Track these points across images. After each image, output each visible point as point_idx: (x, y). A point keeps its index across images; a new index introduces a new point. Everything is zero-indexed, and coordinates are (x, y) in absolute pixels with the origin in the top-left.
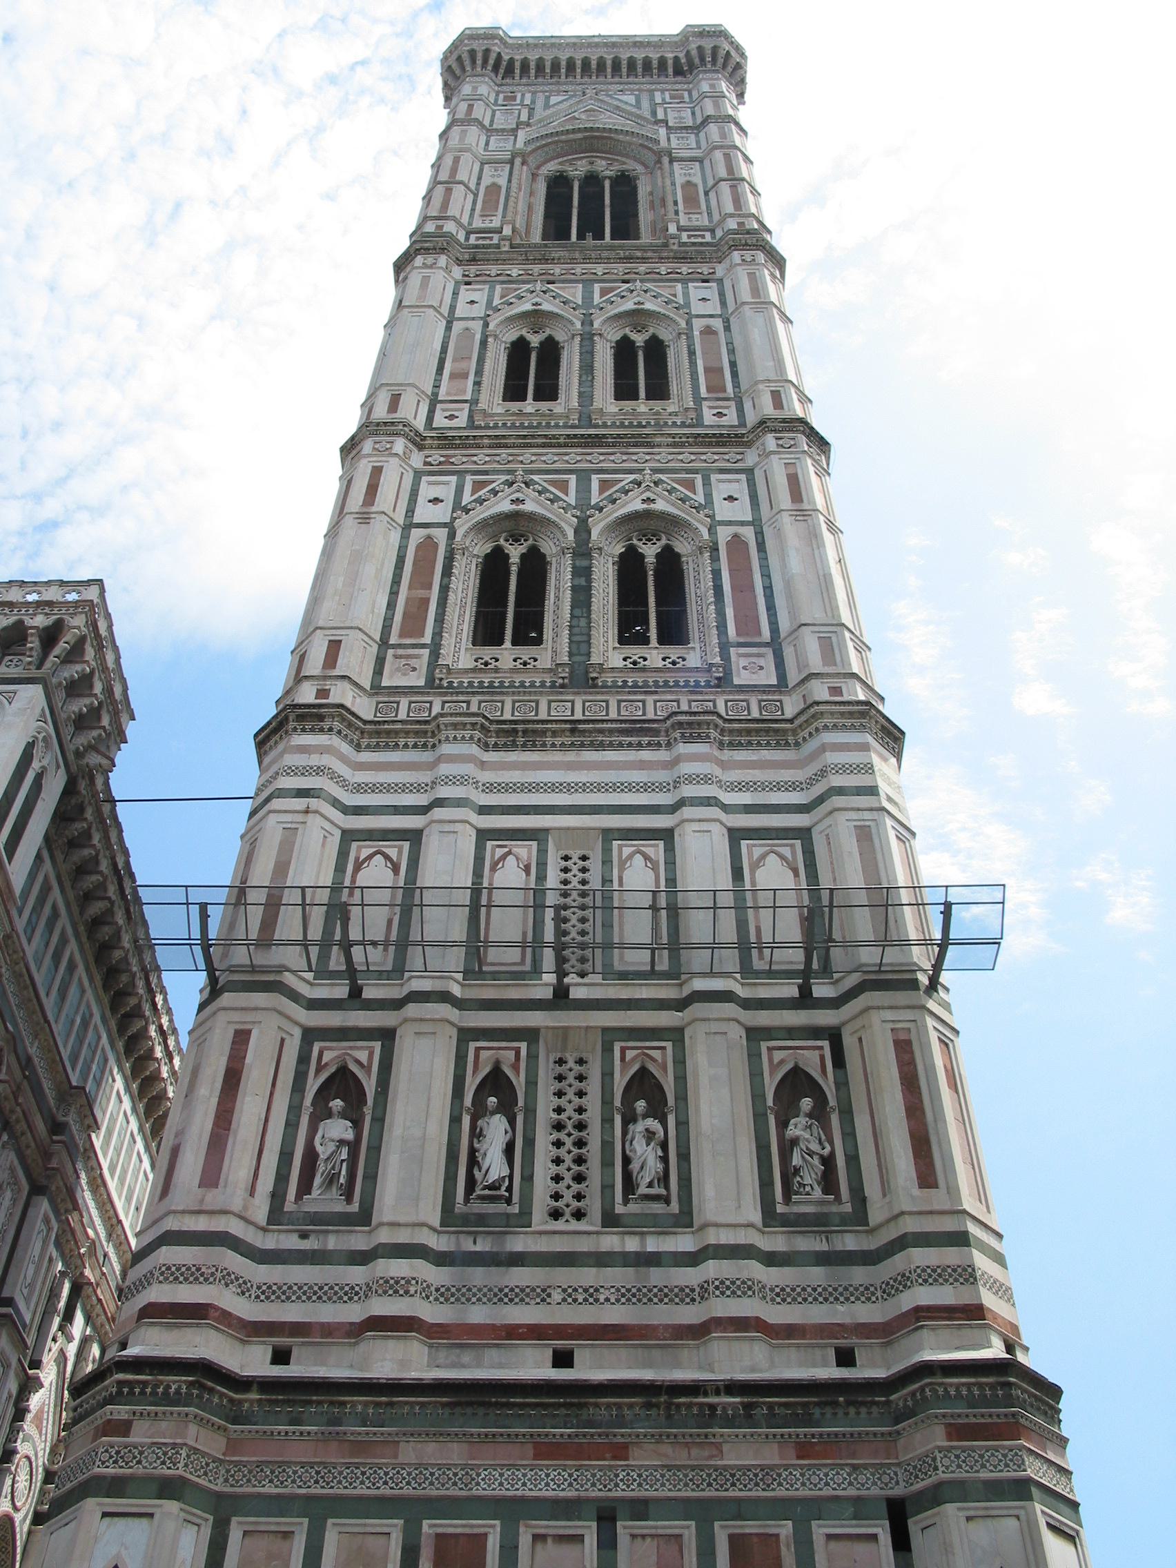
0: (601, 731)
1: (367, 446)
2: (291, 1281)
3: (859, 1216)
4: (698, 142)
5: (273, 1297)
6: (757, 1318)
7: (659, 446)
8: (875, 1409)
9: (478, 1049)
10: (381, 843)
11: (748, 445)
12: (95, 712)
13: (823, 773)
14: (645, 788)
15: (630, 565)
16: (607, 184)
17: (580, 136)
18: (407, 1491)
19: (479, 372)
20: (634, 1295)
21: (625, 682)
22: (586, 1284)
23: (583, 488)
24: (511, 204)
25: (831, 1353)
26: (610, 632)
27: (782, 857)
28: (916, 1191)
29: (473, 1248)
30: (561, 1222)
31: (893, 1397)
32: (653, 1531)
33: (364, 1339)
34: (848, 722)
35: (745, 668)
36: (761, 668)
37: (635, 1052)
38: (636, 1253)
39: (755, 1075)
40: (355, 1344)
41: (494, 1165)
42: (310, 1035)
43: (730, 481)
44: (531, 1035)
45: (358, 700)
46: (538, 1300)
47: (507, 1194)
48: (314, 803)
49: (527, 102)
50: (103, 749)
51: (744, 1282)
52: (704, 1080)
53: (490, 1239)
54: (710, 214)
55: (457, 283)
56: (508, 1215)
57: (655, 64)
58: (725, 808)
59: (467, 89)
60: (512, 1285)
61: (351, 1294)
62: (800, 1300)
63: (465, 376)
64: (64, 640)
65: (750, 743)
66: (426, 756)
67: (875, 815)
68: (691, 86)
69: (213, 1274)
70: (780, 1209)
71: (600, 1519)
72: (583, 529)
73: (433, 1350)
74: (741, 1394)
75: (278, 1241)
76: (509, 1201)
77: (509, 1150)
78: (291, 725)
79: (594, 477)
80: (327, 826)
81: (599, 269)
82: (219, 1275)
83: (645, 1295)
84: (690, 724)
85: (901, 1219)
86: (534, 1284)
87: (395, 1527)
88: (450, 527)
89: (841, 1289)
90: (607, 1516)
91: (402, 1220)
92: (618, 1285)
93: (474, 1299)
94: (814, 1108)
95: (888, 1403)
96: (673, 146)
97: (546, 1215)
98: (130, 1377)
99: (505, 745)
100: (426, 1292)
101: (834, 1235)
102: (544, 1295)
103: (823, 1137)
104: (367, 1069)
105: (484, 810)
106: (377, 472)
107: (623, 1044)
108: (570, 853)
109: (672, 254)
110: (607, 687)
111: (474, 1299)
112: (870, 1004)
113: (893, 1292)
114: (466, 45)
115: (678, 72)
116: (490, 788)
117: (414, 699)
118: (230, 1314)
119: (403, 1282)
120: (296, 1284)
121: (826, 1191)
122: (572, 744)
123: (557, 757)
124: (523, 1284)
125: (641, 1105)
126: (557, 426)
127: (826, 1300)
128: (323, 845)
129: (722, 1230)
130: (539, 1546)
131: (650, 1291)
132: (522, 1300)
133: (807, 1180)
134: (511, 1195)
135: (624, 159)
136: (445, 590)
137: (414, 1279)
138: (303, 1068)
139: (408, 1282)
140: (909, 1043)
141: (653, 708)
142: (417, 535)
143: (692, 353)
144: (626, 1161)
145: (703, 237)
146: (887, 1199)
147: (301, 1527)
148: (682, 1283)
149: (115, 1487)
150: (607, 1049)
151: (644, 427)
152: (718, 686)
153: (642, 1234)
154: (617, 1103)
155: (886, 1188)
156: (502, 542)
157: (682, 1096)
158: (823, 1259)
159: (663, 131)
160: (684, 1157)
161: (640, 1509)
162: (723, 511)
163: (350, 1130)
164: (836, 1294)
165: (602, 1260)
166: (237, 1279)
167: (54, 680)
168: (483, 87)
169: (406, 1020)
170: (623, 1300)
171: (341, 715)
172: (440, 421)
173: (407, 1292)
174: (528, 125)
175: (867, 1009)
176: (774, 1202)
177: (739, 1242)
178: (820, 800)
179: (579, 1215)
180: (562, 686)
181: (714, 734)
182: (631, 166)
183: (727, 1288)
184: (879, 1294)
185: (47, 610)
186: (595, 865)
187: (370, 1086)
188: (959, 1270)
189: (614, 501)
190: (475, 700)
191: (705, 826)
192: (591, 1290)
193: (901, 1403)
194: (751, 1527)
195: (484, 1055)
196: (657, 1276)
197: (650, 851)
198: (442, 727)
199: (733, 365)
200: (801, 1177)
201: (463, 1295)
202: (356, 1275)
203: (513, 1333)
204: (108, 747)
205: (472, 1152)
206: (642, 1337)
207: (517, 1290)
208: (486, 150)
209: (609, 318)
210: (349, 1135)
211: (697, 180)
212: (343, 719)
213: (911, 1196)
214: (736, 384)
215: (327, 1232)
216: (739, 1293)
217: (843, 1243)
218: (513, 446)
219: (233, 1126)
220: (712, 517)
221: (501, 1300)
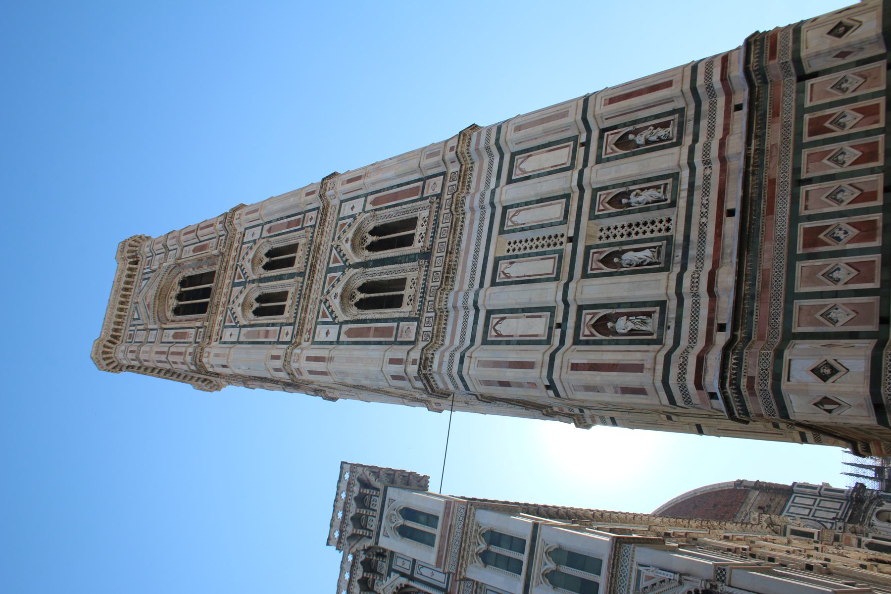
3: (681, 111)
7: (321, 241)
8: (761, 92)
10: (490, 327)
11: (328, 204)
14: (482, 220)
16: (183, 289)
17: (157, 302)
18: (784, 262)
19: (268, 325)
27: (522, 162)
28: (673, 87)
29: (680, 257)
30: (671, 227)
31: (756, 85)
32: (806, 165)
33: (717, 292)
37: (601, 206)
38: (688, 191)
39: (617, 158)
42: (576, 342)
44: (588, 249)
52: (617, 175)
53: (676, 251)
56: (667, 244)
57: (130, 273)
58: (497, 186)
59: (120, 355)
60: (697, 238)
61: (696, 305)
63: (267, 331)
64: (368, 476)
65: (469, 182)
66: (452, 314)
68: (145, 257)
69: (684, 358)
70: (675, 140)
71: (800, 185)
72: (356, 266)
74: (751, 141)
76: (660, 246)
79: (330, 266)
80: (479, 349)
84: (456, 204)
85: (684, 91)
86: (698, 229)
87: (799, 265)
88: (341, 324)
90: (798, 182)
95: (758, 87)
98: (728, 380)
99: (452, 281)
100: (699, 269)
104: (595, 314)
105: (481, 285)
106: (309, 359)
107: (596, 211)
108: (506, 249)
109: (228, 250)
110: (432, 244)
111: (703, 252)
112: (592, 115)
114: (99, 356)
115: (136, 263)
116: (471, 285)
122: (457, 253)
123: (461, 259)
124: (697, 233)
129: (681, 158)
130: (809, 208)
132: (704, 233)
134: (656, 246)
140: (610, 99)
146: (674, 99)
147: (797, 303)
149: (777, 378)
152: (440, 199)
153: (680, 191)
155: (670, 100)
156: (353, 303)
157: (623, 185)
159: (165, 264)
160: (649, 180)
161: (796, 170)
163: (622, 318)
168: (121, 353)
169: (575, 300)
171: (427, 350)
173: (698, 278)
175: (594, 116)
178: (499, 149)
179: (669, 220)
180: (429, 262)
184: (713, 99)
187: (603, 312)
190: (428, 298)
193: (759, 81)
194: (806, 129)
195: (594, 266)
196: (699, 182)
197: (511, 214)
198: (440, 307)
199: (288, 217)
202: (688, 303)
203: (718, 235)
205: (637, 266)
206: (724, 184)
209: (253, 273)
210: (625, 317)
211: (193, 247)
214: (299, 214)
215: (667, 318)
217: (692, 115)
219: (616, 362)
220: (360, 213)
221: (704, 242)
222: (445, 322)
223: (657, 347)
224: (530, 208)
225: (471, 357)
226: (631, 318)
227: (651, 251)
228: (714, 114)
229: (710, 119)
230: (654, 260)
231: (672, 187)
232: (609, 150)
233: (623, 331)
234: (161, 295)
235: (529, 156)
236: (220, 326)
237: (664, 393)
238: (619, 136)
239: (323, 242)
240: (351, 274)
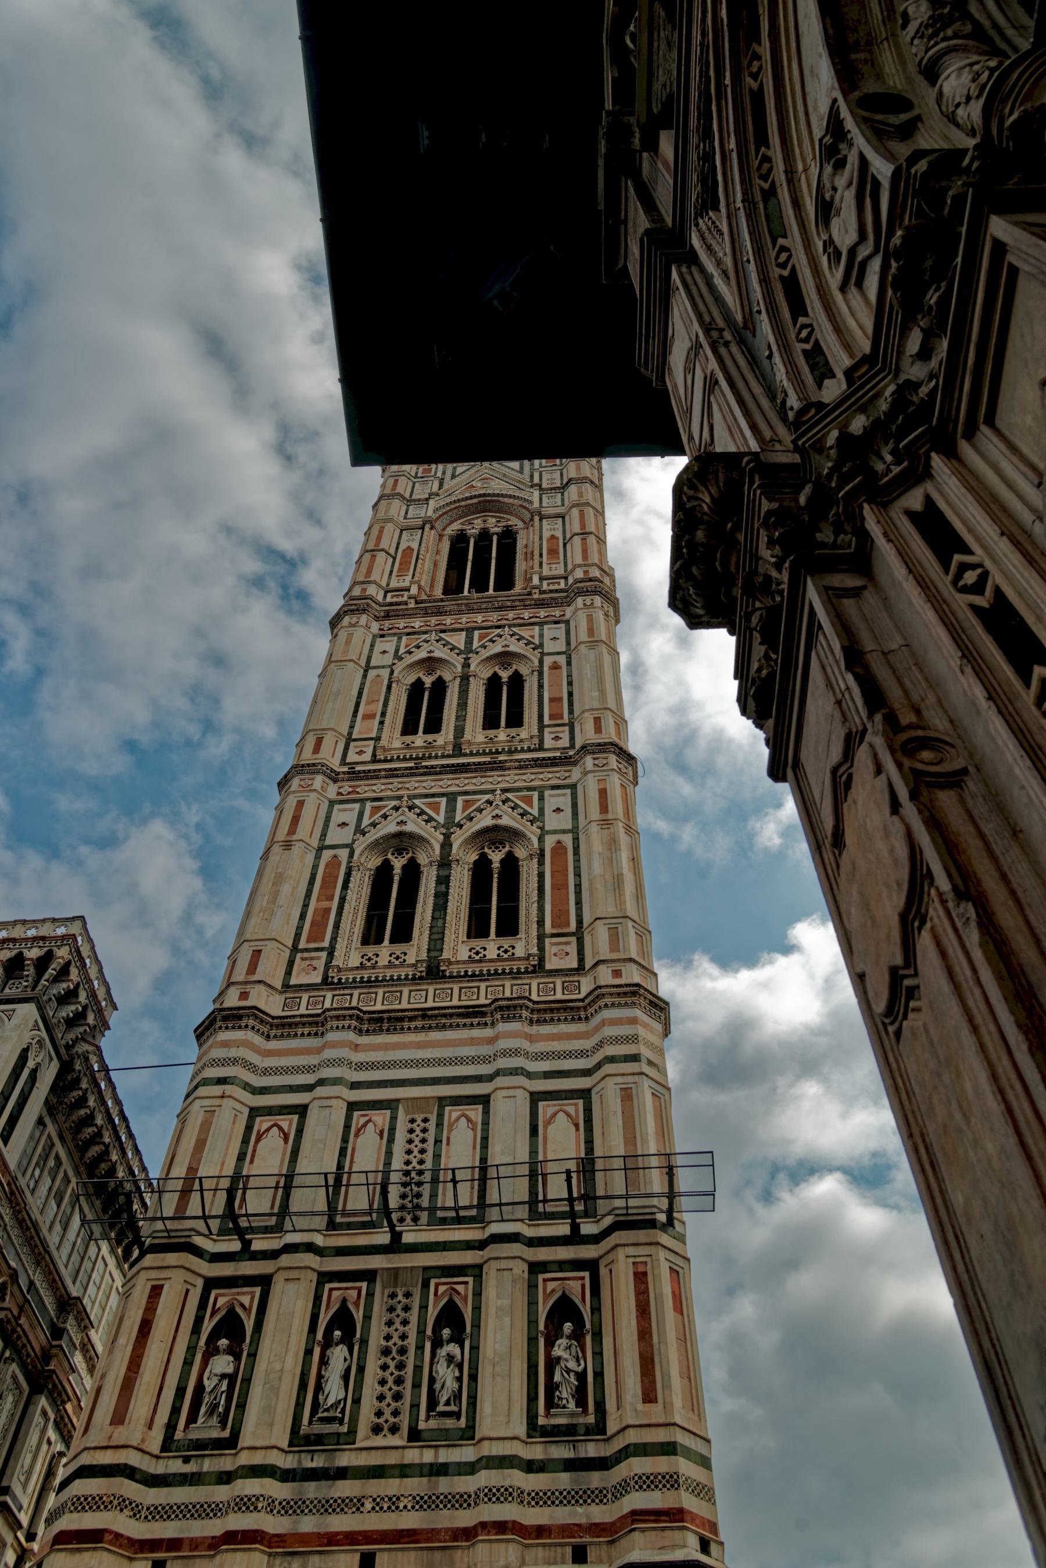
0: (445, 1016)
1: (295, 783)
2: (172, 1502)
3: (599, 1428)
4: (563, 500)
6: (514, 1522)
7: (509, 769)
9: (331, 1290)
11: (575, 764)
12: (81, 1016)
13: (600, 1045)
14: (474, 1060)
15: (481, 869)
16: (495, 538)
17: (475, 501)
21: (466, 972)
22: (390, 1493)
23: (451, 809)
24: (419, 565)
25: (569, 1550)
26: (461, 928)
27: (568, 1115)
28: (640, 1407)
34: (623, 1000)
35: (555, 955)
36: (567, 954)
38: (431, 1465)
39: (532, 1303)
40: (214, 1556)
41: (334, 1390)
43: (559, 795)
44: (369, 1276)
45: (271, 998)
46: (354, 1509)
48: (228, 1089)
49: (439, 474)
50: (90, 1039)
51: (506, 1490)
52: (492, 1311)
53: (324, 1455)
54: (565, 565)
55: (375, 637)
56: (338, 1434)
60: (336, 1496)
65: (552, 1020)
67: (636, 1078)
69: (111, 1502)
70: (541, 1421)
72: (446, 845)
75: (166, 1467)
76: (341, 1421)
77: (346, 1377)
78: (218, 1024)
80: (238, 1106)
81: (479, 618)
82: (115, 1502)
84: (508, 1007)
85: (627, 1431)
86: (352, 1495)
88: (350, 847)
89: (581, 1493)
91: (258, 1444)
92: (414, 1494)
94: (573, 1331)
96: (544, 504)
99: (374, 1030)
100: (272, 1506)
103: (580, 1355)
105: (355, 1086)
106: (301, 804)
108: (416, 1116)
112: (619, 1242)
116: (361, 1066)
117: (312, 994)
118: (122, 1536)
122: (423, 1027)
123: (411, 1037)
124: (345, 1495)
125: (446, 1332)
126: (436, 757)
127: (569, 1502)
128: (234, 1122)
129: (494, 1442)
131: (438, 1498)
132: (342, 1510)
133: (564, 1395)
135: (509, 517)
136: (343, 900)
138: (201, 1313)
140: (645, 1274)
141: (483, 995)
142: (327, 855)
143: (541, 686)
144: (432, 1380)
145: (559, 584)
148: (462, 1490)
150: (426, 1285)
151: (500, 753)
152: (533, 972)
153: (437, 1446)
154: (429, 1332)
156: (390, 856)
157: (476, 1325)
158: (571, 1465)
159: (536, 493)
160: (474, 1377)
162: (552, 821)
163: (232, 1366)
165: (404, 1471)
166: (131, 1504)
167: (45, 998)
170: (417, 1507)
172: (352, 757)
173: (256, 1508)
174: (438, 495)
175: (616, 1246)
176: (536, 1416)
178: (599, 1066)
179: (394, 1429)
180: (421, 978)
181: (525, 1013)
182: (514, 521)
183: (495, 1495)
184: (609, 1496)
185: (41, 944)
186: (432, 1126)
187: (249, 1325)
189: (471, 819)
191: (511, 1092)
192: (394, 1499)
196: (444, 1485)
197: (472, 1114)
199: (570, 694)
202: (221, 1493)
204: (94, 1037)
205: (320, 1377)
208: (405, 518)
212: (256, 1017)
214: (571, 711)
215: (204, 1456)
217: (586, 1451)
218: (403, 776)
219: (141, 1370)
220: (542, 828)
222: (306, 1033)
224: (474, 1148)
225: (223, 1097)
227: (340, 1401)
228: (577, 1501)
229: (569, 1493)
231: (447, 1430)
233: (206, 1375)
234: (487, 504)
235: (577, 1126)
236: (405, 627)
238: (578, 1301)
239: (507, 772)
240: (433, 841)
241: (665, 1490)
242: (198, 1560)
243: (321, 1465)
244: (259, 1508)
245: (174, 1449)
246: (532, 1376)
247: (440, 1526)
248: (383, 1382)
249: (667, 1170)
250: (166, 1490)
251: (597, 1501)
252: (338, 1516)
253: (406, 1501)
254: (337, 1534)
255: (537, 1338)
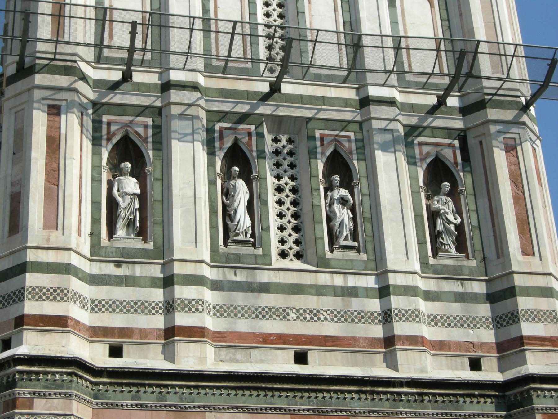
2: (114, 298)
5: (103, 309)
20: (342, 316)
22: (311, 307)
25: (466, 361)
30: (287, 260)
31: (507, 393)
38: (342, 287)
47: (252, 240)
51: (413, 312)
56: (256, 256)
60: (263, 305)
62: (446, 324)
70: (432, 261)
73: (217, 349)
75: (100, 268)
83: (349, 316)
86: (278, 306)
89: (471, 319)
92: (332, 309)
93: (239, 315)
97: (277, 255)
101: (466, 282)
102: (285, 314)
111: (239, 315)
113: (505, 324)
118: (79, 322)
119: (193, 302)
120: (118, 300)
121: (458, 250)
124: (271, 305)
127: (462, 325)
129: (397, 274)
131: (352, 314)
132: (271, 317)
137: (201, 300)
138: (97, 135)
139: (197, 302)
144: (330, 219)
146: (501, 260)
164: (468, 322)
170: (336, 319)
173: (197, 310)
176: (427, 256)
177: (408, 284)
188: (548, 313)
192: (315, 312)
193: (512, 398)
196: (356, 304)
200: (443, 239)
201: (232, 312)
205: (224, 206)
206: (349, 345)
207: (267, 310)
210: (138, 191)
213: (518, 261)
216: (410, 319)
217: (472, 288)
221: (257, 316)
223: (87, 252)
224: (336, 10)
226: (137, 201)
228: (469, 325)
229: (461, 318)
230: (231, 235)
231: (352, 261)
232: (425, 149)
237: (11, 266)
241: (546, 323)
242: (151, 346)
243: (244, 279)
244: (201, 309)
245: (103, 254)
246: (419, 225)
247: (358, 336)
248: (281, 215)
249: (549, 62)
250: (105, 288)
251: (485, 326)
252: (268, 321)
253: (324, 313)
254: (270, 335)
255: (419, 192)
